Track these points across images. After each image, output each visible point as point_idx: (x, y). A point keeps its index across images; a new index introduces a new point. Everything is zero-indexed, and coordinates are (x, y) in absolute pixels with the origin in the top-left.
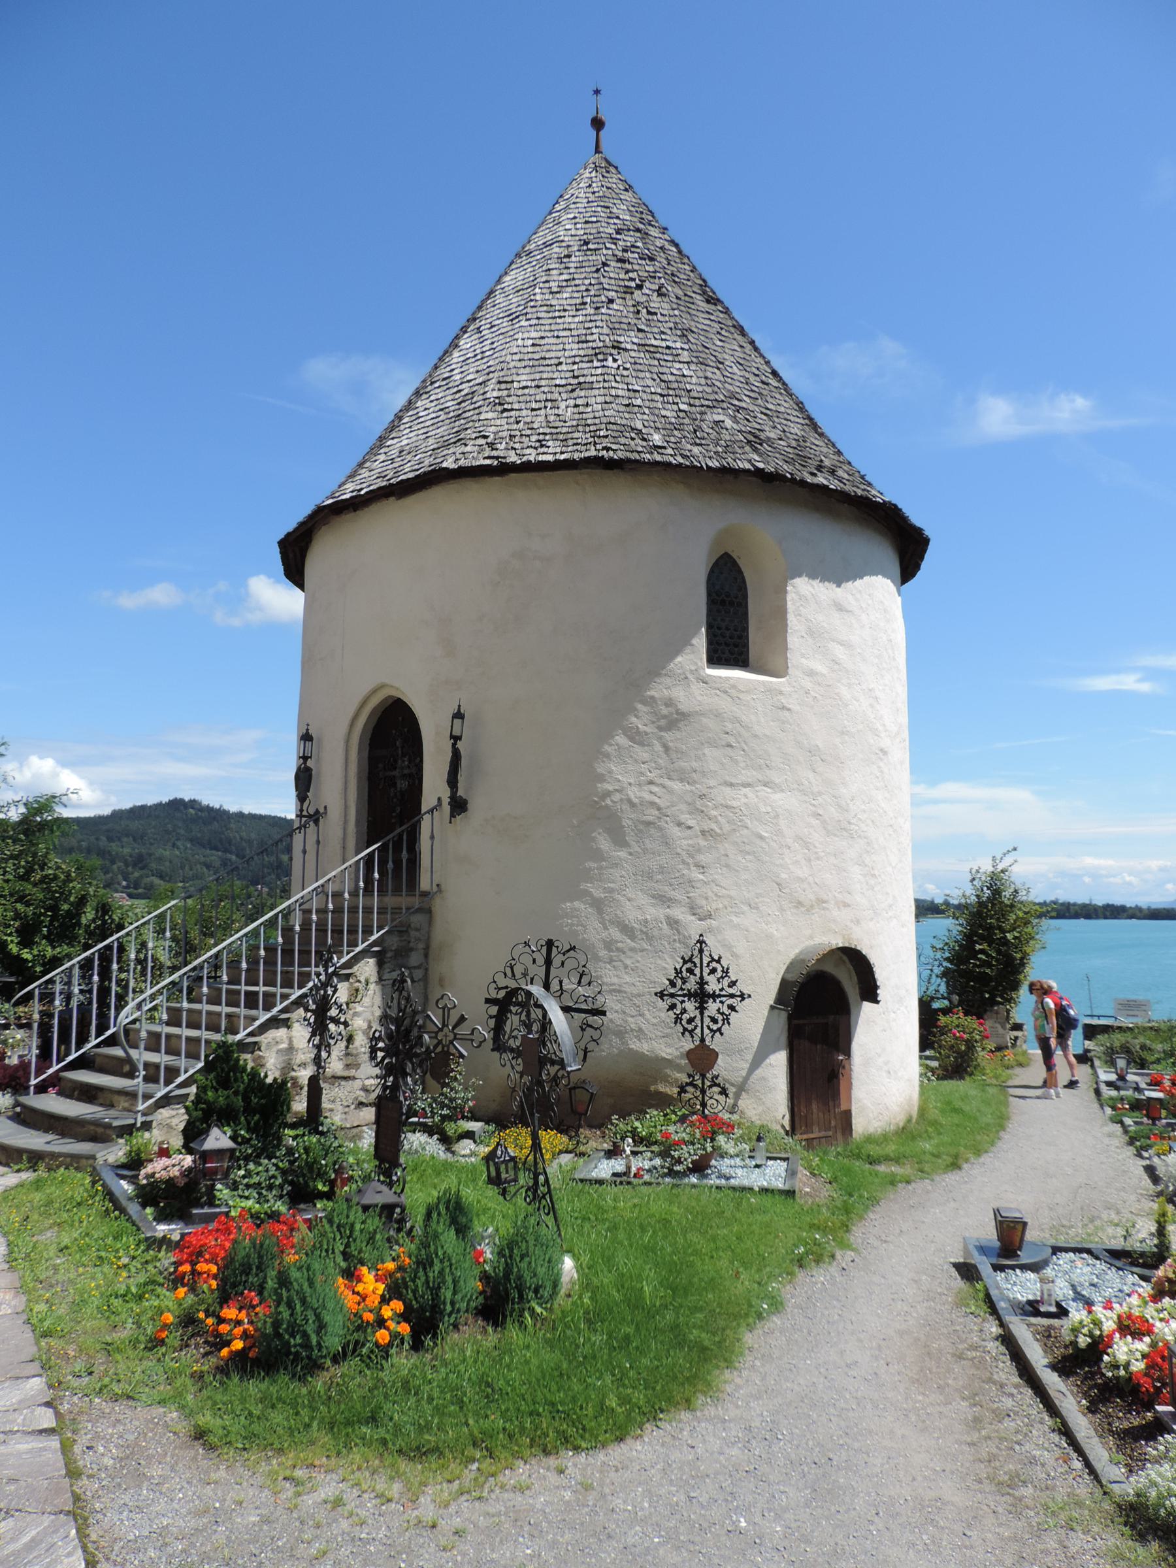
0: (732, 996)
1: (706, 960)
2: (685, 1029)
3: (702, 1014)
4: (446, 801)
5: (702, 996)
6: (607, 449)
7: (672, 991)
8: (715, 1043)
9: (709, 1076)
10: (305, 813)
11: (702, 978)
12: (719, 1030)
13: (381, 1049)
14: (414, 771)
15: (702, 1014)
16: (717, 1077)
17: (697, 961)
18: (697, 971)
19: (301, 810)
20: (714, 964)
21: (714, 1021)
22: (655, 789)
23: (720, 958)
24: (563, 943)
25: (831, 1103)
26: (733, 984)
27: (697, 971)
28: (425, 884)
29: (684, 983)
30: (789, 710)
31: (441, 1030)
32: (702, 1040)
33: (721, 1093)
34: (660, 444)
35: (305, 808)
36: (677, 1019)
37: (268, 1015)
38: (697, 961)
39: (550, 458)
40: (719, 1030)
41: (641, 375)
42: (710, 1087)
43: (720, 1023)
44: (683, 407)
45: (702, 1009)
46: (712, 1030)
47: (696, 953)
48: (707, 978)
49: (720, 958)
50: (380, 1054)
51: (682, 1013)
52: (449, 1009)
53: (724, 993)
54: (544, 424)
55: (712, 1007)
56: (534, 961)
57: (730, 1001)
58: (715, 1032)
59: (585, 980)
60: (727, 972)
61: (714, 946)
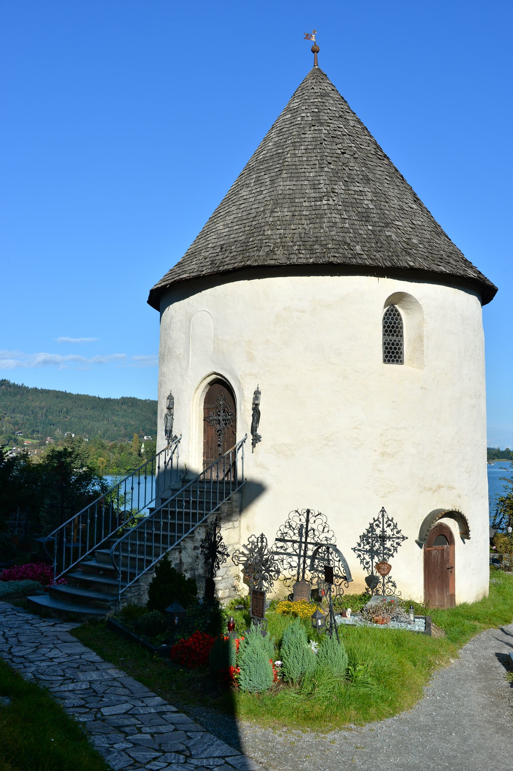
0: (398, 538)
1: (385, 520)
8: (390, 561)
9: (386, 577)
11: (383, 529)
16: (390, 577)
17: (381, 520)
18: (381, 525)
20: (390, 522)
23: (392, 519)
24: (315, 511)
27: (381, 525)
33: (392, 586)
34: (360, 252)
37: (172, 547)
38: (381, 520)
39: (304, 261)
41: (347, 209)
42: (387, 583)
43: (393, 551)
44: (370, 228)
47: (380, 516)
48: (386, 529)
49: (392, 519)
53: (394, 536)
54: (299, 239)
56: (300, 520)
57: (398, 541)
59: (326, 530)
60: (396, 526)
61: (389, 514)
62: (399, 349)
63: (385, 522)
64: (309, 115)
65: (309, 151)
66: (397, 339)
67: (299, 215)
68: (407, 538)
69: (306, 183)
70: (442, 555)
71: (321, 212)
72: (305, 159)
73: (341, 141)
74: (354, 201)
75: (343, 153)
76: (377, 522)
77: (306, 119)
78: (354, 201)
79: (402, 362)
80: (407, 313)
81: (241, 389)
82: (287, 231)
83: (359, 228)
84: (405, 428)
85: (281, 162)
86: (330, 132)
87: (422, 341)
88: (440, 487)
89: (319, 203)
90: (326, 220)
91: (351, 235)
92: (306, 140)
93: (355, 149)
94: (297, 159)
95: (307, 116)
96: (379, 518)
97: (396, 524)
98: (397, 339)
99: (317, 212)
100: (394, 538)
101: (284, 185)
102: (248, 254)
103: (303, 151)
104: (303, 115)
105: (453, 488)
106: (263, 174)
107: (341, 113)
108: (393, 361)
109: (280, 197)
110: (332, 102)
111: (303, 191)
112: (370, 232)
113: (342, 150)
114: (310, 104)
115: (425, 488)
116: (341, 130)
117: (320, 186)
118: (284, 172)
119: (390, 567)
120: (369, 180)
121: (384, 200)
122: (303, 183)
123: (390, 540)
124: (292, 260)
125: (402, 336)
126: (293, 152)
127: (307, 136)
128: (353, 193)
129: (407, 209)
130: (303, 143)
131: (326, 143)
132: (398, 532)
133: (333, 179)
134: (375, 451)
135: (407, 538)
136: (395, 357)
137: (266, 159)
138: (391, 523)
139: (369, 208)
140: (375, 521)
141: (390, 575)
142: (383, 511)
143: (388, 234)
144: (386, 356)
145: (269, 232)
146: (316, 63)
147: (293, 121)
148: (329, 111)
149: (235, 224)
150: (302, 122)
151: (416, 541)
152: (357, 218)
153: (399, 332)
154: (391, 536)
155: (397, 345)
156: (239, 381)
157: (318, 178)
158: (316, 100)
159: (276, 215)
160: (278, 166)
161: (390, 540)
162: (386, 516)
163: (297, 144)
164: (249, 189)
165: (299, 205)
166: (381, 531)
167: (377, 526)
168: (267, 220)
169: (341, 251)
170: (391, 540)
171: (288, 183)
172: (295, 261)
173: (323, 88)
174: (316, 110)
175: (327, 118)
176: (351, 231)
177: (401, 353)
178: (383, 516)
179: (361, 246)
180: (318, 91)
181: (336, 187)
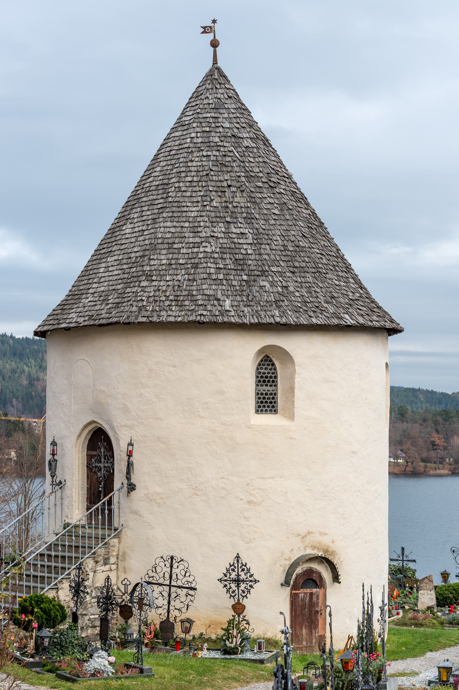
0: (251, 581)
1: (240, 565)
2: (231, 596)
3: (238, 589)
4: (126, 486)
5: (238, 581)
7: (226, 578)
8: (245, 602)
9: (241, 616)
10: (54, 483)
12: (246, 596)
13: (101, 602)
14: (110, 465)
15: (238, 589)
16: (245, 616)
17: (236, 565)
18: (236, 570)
19: (53, 482)
20: (243, 567)
22: (224, 480)
23: (246, 564)
24: (178, 556)
25: (313, 631)
26: (251, 576)
27: (236, 570)
28: (116, 524)
29: (230, 575)
30: (295, 439)
31: (124, 594)
32: (239, 600)
33: (246, 624)
35: (54, 480)
36: (227, 591)
38: (236, 565)
39: (172, 319)
40: (246, 596)
41: (225, 256)
42: (242, 621)
43: (246, 593)
44: (245, 277)
45: (238, 586)
46: (242, 596)
47: (235, 562)
50: (101, 604)
51: (230, 589)
52: (127, 585)
53: (248, 580)
57: (251, 583)
58: (244, 597)
60: (249, 571)
62: (273, 398)
63: (239, 567)
65: (195, 184)
67: (175, 264)
68: (259, 581)
69: (187, 224)
71: (196, 261)
72: (189, 194)
73: (229, 169)
75: (229, 186)
76: (233, 567)
79: (276, 412)
80: (281, 363)
82: (162, 283)
83: (232, 278)
84: (272, 478)
85: (165, 195)
86: (219, 158)
89: (196, 250)
92: (192, 169)
93: (243, 179)
95: (197, 137)
96: (234, 563)
97: (249, 569)
99: (193, 261)
100: (248, 581)
102: (122, 308)
103: (188, 184)
104: (193, 135)
107: (235, 130)
108: (266, 411)
112: (244, 283)
113: (229, 182)
115: (293, 534)
116: (231, 154)
117: (199, 229)
119: (244, 607)
120: (253, 219)
122: (182, 224)
123: (244, 583)
124: (161, 318)
125: (276, 386)
126: (177, 185)
127: (195, 164)
128: (234, 236)
129: (291, 249)
130: (189, 174)
131: (212, 173)
133: (214, 220)
134: (241, 499)
135: (259, 581)
137: (152, 188)
138: (245, 568)
139: (247, 254)
140: (231, 566)
141: (244, 614)
142: (238, 557)
143: (262, 283)
144: (259, 407)
145: (144, 284)
148: (221, 129)
152: (233, 267)
154: (245, 579)
156: (116, 432)
157: (199, 219)
158: (209, 115)
159: (152, 263)
161: (244, 583)
162: (240, 562)
165: (176, 251)
166: (236, 575)
167: (233, 570)
169: (209, 307)
170: (245, 583)
171: (169, 224)
172: (164, 319)
174: (208, 129)
175: (217, 139)
176: (225, 282)
178: (238, 561)
179: (232, 301)
181: (215, 230)
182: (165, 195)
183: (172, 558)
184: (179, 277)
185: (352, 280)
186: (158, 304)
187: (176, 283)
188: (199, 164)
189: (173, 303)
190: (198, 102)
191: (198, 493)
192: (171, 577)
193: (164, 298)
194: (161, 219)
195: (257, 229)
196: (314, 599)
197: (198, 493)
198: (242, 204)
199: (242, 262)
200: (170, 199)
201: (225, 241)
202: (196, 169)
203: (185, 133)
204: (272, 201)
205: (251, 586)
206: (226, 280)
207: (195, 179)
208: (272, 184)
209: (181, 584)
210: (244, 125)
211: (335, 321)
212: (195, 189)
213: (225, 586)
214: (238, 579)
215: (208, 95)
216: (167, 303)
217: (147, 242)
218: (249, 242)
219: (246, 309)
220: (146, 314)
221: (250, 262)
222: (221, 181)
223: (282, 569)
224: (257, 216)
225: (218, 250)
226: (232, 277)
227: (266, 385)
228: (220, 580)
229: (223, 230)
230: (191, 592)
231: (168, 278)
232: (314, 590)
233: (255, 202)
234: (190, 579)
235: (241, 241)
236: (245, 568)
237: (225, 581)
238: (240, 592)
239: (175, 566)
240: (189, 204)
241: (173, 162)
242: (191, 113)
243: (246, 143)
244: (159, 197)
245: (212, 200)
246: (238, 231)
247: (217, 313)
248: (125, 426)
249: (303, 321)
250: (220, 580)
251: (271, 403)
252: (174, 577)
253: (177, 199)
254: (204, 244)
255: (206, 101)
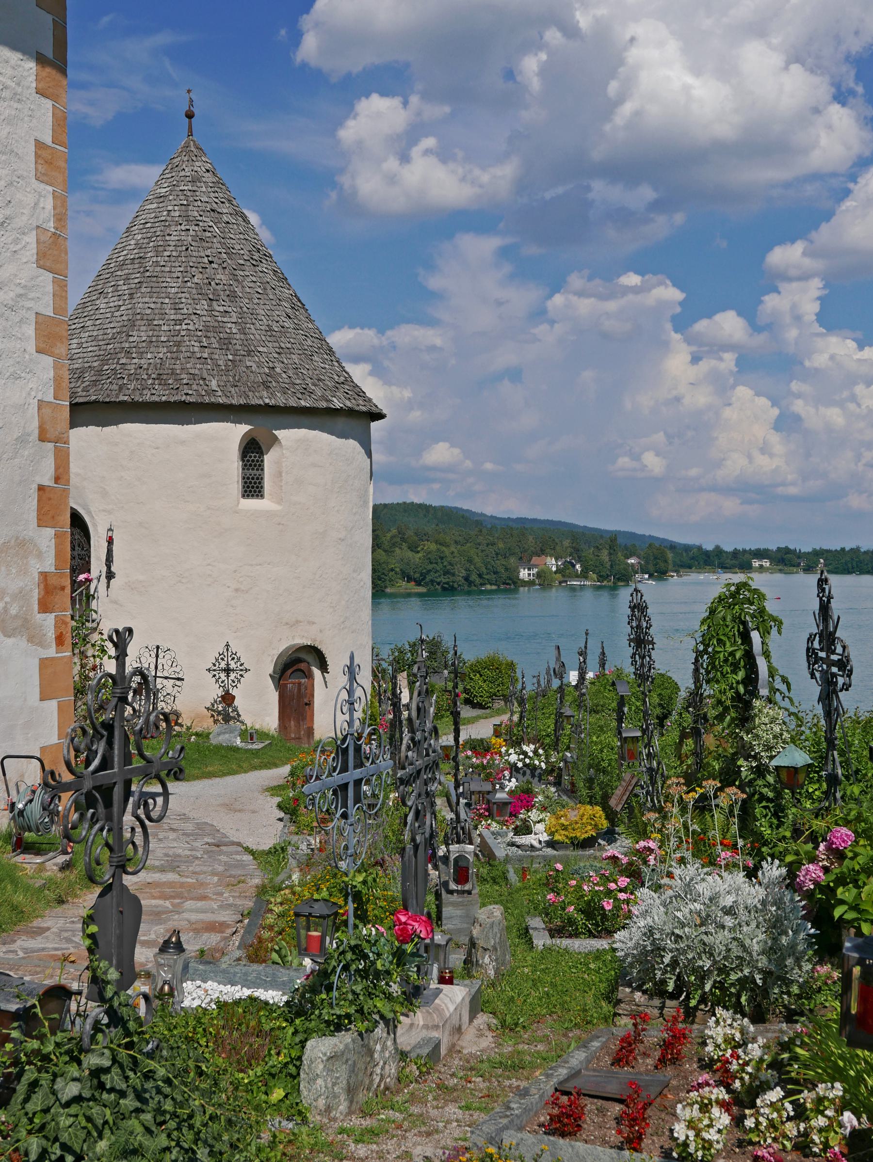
0: (242, 670)
1: (230, 654)
5: (228, 671)
6: (187, 394)
8: (234, 692)
21: (234, 682)
22: (210, 567)
24: (164, 646)
25: (301, 723)
39: (155, 398)
44: (230, 357)
45: (228, 676)
55: (232, 676)
62: (260, 483)
64: (176, 208)
66: (258, 473)
69: (167, 301)
70: (299, 689)
71: (179, 338)
72: (167, 269)
73: (210, 245)
74: (216, 324)
75: (211, 262)
77: (172, 214)
78: (216, 324)
79: (262, 496)
81: (95, 525)
82: (143, 361)
85: (142, 270)
86: (199, 233)
87: (281, 476)
88: (298, 622)
89: (178, 327)
90: (184, 349)
91: (209, 367)
93: (225, 256)
94: (158, 269)
98: (258, 473)
99: (175, 339)
101: (144, 303)
103: (167, 259)
104: (170, 208)
105: (314, 623)
106: (121, 282)
107: (215, 205)
108: (253, 496)
109: (139, 317)
110: (204, 189)
111: (163, 311)
113: (210, 259)
114: (180, 193)
117: (181, 306)
118: (145, 285)
119: (234, 697)
121: (250, 321)
122: (162, 300)
125: (262, 470)
126: (155, 259)
127: (172, 238)
128: (217, 314)
130: (167, 248)
132: (241, 665)
133: (196, 297)
136: (255, 492)
137: (127, 262)
142: (227, 645)
143: (248, 364)
144: (246, 491)
146: (190, 133)
147: (159, 215)
149: (89, 344)
150: (169, 219)
151: (270, 675)
153: (260, 465)
155: (258, 479)
157: (180, 295)
158: (186, 188)
159: (131, 339)
160: (138, 275)
163: (161, 249)
164: (106, 300)
167: (223, 659)
168: (123, 345)
171: (146, 300)
173: (195, 169)
174: (185, 203)
175: (196, 214)
177: (262, 487)
178: (227, 650)
180: (188, 174)
181: (198, 307)
182: (142, 270)
183: (158, 647)
184: (161, 355)
185: (336, 364)
186: (139, 382)
187: (159, 361)
188: (177, 238)
189: (156, 382)
190: (174, 174)
191: (184, 581)
192: (156, 668)
193: (146, 377)
194: (139, 295)
195: (241, 308)
196: (303, 690)
197: (184, 581)
198: (225, 282)
199: (226, 342)
200: (148, 274)
201: (209, 319)
202: (174, 243)
203: (161, 205)
204: (254, 279)
205: (241, 676)
206: (211, 359)
207: (174, 254)
208: (254, 262)
209: (167, 675)
210: (223, 200)
211: (324, 404)
212: (174, 264)
213: (214, 676)
214: (227, 668)
215: (184, 166)
216: (150, 382)
217: (124, 318)
218: (233, 321)
219: (233, 390)
220: (127, 392)
221: (235, 341)
222: (201, 257)
223: (270, 658)
224: (240, 295)
225: (201, 328)
226: (217, 357)
227: (253, 469)
228: (209, 670)
229: (206, 307)
230: (178, 683)
231: (149, 356)
232: (303, 681)
233: (237, 280)
234: (178, 670)
235: (225, 320)
236: (234, 656)
237: (214, 670)
238: (230, 682)
239: (161, 656)
240: (169, 280)
241: (149, 235)
242: (166, 185)
243: (225, 218)
244: (136, 271)
245: (194, 276)
246: (221, 309)
247: (204, 393)
248: (104, 511)
249: (293, 403)
250: (209, 670)
251: (257, 487)
252: (160, 667)
253: (155, 274)
254: (186, 321)
255: (183, 173)
